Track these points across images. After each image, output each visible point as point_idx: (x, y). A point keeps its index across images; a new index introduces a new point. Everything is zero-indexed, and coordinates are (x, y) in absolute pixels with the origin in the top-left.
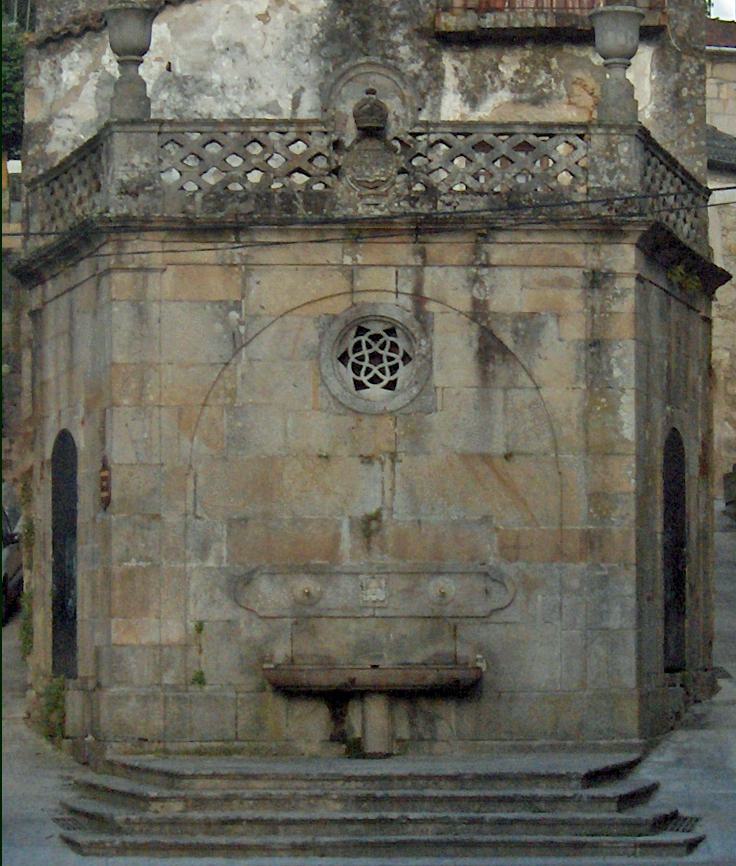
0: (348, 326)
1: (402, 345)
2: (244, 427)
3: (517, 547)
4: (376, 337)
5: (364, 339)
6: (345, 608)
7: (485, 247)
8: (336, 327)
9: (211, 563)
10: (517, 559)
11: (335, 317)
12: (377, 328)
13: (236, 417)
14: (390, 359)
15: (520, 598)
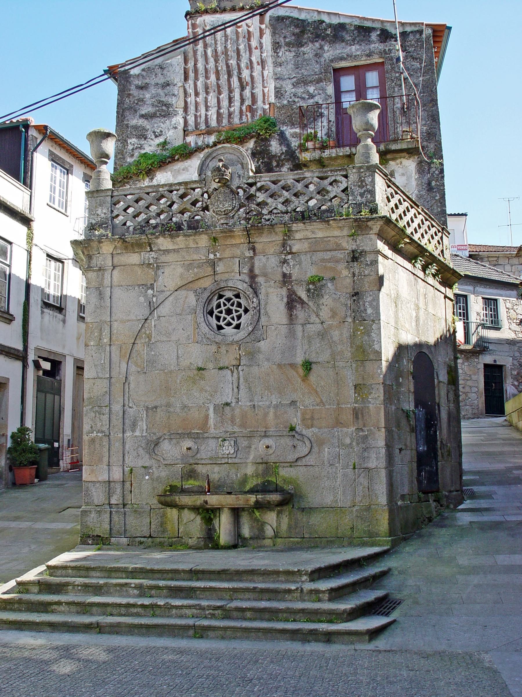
0: (213, 294)
1: (242, 301)
2: (155, 355)
3: (312, 418)
4: (229, 300)
5: (222, 301)
6: (211, 458)
7: (289, 242)
8: (206, 295)
9: (137, 433)
10: (312, 426)
11: (205, 289)
12: (229, 294)
13: (151, 350)
14: (237, 311)
15: (315, 449)
